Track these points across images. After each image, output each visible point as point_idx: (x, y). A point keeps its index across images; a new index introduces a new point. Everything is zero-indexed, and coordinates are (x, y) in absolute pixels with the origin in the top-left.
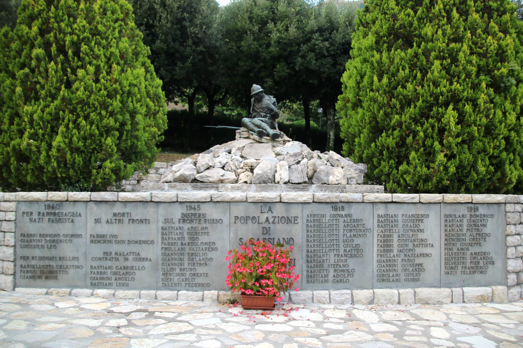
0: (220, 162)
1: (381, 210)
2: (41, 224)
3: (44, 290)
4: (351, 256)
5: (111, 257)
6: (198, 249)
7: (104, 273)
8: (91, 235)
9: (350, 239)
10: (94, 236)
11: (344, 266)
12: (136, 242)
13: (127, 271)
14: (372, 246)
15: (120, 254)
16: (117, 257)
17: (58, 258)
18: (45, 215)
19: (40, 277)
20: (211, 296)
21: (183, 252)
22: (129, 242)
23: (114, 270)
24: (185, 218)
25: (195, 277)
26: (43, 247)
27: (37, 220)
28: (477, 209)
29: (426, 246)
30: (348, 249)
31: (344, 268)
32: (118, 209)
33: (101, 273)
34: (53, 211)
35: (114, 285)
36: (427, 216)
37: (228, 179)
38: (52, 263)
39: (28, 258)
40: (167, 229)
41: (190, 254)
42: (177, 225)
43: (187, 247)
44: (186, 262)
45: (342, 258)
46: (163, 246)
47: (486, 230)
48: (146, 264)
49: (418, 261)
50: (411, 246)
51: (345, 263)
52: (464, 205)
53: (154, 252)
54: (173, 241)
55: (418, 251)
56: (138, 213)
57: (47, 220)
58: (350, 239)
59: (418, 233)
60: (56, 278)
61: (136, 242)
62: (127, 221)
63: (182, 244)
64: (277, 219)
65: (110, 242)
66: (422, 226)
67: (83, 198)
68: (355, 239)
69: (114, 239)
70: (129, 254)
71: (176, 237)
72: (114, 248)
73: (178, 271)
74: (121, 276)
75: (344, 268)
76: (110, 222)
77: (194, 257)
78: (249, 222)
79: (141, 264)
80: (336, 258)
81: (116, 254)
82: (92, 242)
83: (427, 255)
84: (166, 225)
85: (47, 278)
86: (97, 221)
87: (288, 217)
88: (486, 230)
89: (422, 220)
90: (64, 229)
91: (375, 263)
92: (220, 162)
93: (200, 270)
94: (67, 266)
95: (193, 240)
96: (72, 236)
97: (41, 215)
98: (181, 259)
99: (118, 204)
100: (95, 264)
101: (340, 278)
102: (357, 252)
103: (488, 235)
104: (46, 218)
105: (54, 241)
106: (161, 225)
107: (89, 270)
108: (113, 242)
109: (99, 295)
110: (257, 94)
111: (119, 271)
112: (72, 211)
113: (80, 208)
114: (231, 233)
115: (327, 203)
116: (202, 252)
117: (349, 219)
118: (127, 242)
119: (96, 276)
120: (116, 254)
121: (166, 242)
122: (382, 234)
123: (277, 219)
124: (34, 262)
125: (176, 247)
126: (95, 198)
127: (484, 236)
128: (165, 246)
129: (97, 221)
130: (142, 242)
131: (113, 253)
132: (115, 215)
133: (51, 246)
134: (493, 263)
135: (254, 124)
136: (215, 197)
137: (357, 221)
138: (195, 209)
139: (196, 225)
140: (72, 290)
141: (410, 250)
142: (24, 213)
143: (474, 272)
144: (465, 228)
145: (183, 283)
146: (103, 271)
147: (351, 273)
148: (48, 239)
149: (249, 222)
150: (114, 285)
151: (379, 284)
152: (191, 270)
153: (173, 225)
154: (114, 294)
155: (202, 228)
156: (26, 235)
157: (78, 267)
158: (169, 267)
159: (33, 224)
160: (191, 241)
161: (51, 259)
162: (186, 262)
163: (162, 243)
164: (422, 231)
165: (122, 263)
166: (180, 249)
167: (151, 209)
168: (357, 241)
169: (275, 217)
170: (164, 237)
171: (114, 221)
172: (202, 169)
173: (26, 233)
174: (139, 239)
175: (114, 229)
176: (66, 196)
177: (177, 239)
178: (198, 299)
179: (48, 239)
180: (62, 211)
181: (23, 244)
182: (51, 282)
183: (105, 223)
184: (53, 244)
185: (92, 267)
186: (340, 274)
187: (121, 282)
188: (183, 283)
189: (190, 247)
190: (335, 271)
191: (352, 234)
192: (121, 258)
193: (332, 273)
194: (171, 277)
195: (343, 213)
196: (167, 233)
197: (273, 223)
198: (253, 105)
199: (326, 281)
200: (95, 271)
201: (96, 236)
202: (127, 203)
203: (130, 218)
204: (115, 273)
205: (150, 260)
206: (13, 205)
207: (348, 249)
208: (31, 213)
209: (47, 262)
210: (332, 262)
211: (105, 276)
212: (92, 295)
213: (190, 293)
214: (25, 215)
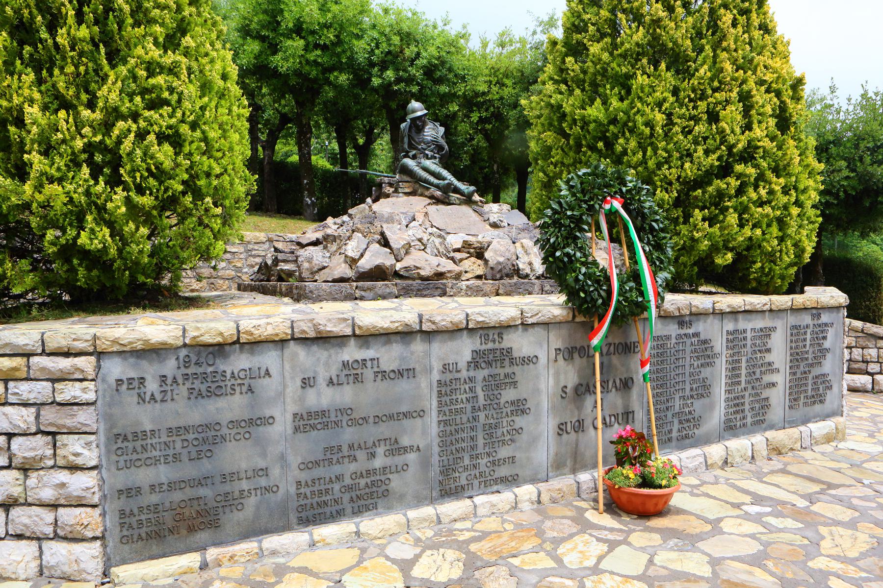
0: (420, 240)
1: (729, 326)
2: (169, 405)
3: (191, 560)
5: (340, 455)
6: (500, 415)
7: (327, 491)
8: (295, 415)
9: (697, 370)
10: (302, 418)
11: (690, 413)
12: (391, 417)
13: (373, 478)
14: (719, 377)
15: (360, 447)
16: (352, 453)
17: (218, 479)
20: (528, 497)
21: (474, 424)
22: (378, 420)
23: (348, 481)
24: (478, 360)
25: (496, 468)
26: (176, 458)
27: (158, 397)
28: (819, 316)
29: (772, 371)
30: (694, 386)
31: (690, 417)
32: (352, 353)
33: (320, 492)
34: (200, 370)
35: (349, 510)
36: (774, 329)
37: (449, 272)
38: (202, 492)
39: (139, 490)
40: (448, 383)
41: (487, 427)
42: (464, 374)
43: (482, 415)
44: (481, 442)
45: (689, 402)
46: (441, 418)
47: (827, 344)
48: (412, 457)
51: (691, 409)
52: (808, 311)
53: (425, 432)
54: (458, 407)
56: (389, 356)
57: (185, 393)
58: (697, 370)
59: (765, 355)
61: (391, 417)
62: (372, 376)
63: (473, 408)
64: (612, 348)
67: (277, 335)
68: (702, 369)
69: (345, 418)
70: (377, 444)
71: (464, 397)
72: (348, 435)
73: (467, 461)
74: (363, 492)
75: (690, 417)
76: (335, 381)
77: (494, 431)
78: (576, 355)
79: (399, 460)
80: (682, 402)
81: (351, 447)
82: (296, 429)
84: (448, 376)
85: (191, 530)
86: (307, 383)
87: (626, 344)
88: (827, 344)
89: (769, 335)
90: (230, 407)
91: (723, 404)
92: (420, 240)
93: (504, 452)
94: (242, 492)
96: (251, 422)
97: (169, 381)
98: (472, 438)
100: (304, 476)
101: (685, 432)
102: (704, 390)
103: (827, 350)
104: (183, 390)
106: (436, 376)
107: (293, 490)
108: (344, 423)
109: (328, 541)
110: (420, 117)
111: (357, 481)
112: (247, 367)
113: (270, 359)
114: (551, 379)
115: (674, 317)
116: (507, 419)
117: (696, 339)
118: (371, 420)
119: (308, 502)
120: (351, 447)
121: (446, 409)
122: (730, 359)
123: (612, 348)
124: (154, 498)
125: (463, 416)
126: (304, 332)
127: (824, 352)
128: (444, 418)
129: (307, 383)
130: (401, 416)
131: (345, 448)
132: (345, 365)
135: (426, 169)
136: (529, 315)
137: (705, 342)
138: (494, 341)
139: (497, 371)
140: (260, 542)
141: (757, 379)
142: (119, 382)
143: (814, 403)
144: (808, 343)
145: (476, 482)
146: (322, 487)
147: (697, 422)
148: (191, 437)
149: (576, 355)
150: (349, 510)
151: (726, 434)
152: (488, 455)
153: (458, 375)
154: (358, 533)
155: (507, 376)
156: (130, 437)
158: (451, 457)
159: (149, 407)
160: (489, 402)
161: (203, 481)
162: (481, 442)
163: (439, 412)
165: (362, 463)
166: (471, 419)
167: (418, 346)
168: (706, 372)
169: (610, 344)
170: (443, 399)
171: (343, 379)
172: (403, 251)
173: (129, 431)
174: (395, 411)
175: (346, 395)
176: (235, 332)
177: (464, 400)
178: (509, 507)
179: (191, 437)
180: (222, 367)
182: (202, 536)
183: (324, 384)
184: (205, 447)
185: (299, 483)
186: (685, 426)
187: (362, 502)
188: (476, 482)
189: (487, 412)
190: (680, 422)
191: (699, 362)
192: (361, 455)
193: (676, 426)
194: (455, 475)
195: (691, 331)
196: (448, 392)
197: (607, 354)
198: (409, 136)
199: (670, 440)
201: (305, 417)
202: (370, 339)
203: (376, 370)
204: (349, 488)
205: (418, 449)
206: (86, 363)
207: (694, 386)
209: (190, 493)
210: (677, 409)
212: (313, 545)
213: (494, 498)
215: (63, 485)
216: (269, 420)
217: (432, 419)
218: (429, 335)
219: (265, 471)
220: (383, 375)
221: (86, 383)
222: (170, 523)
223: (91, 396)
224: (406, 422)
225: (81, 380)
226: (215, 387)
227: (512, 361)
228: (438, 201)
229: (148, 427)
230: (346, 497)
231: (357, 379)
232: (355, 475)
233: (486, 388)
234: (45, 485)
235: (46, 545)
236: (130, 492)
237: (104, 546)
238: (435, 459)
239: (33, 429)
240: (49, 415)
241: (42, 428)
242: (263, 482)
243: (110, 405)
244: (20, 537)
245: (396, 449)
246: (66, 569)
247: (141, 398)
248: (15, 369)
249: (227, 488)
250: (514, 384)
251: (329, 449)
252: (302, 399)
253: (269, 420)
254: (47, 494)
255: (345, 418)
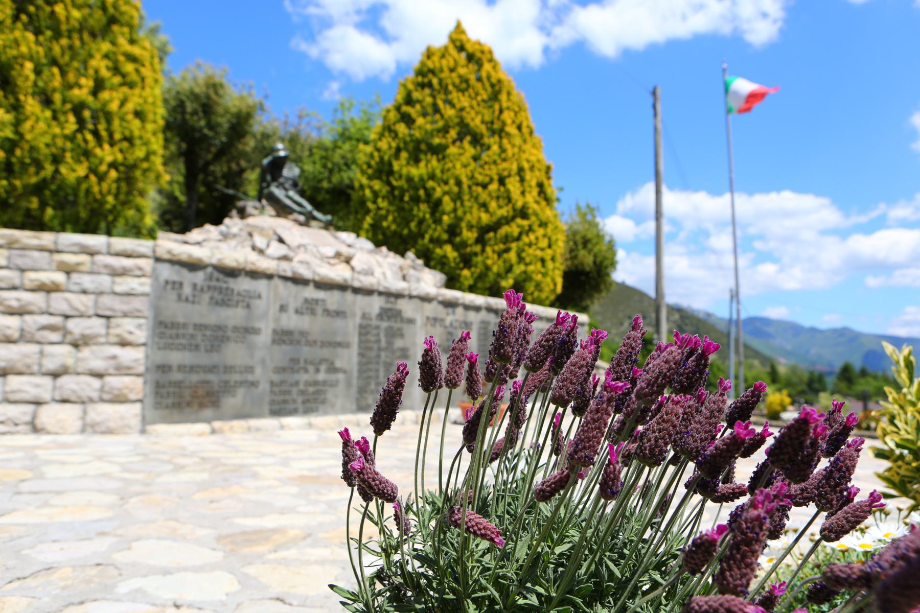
17: (222, 369)
18: (205, 289)
19: (189, 404)
23: (302, 387)
26: (197, 347)
27: (191, 298)
32: (310, 292)
38: (212, 377)
43: (383, 354)
48: (341, 376)
56: (332, 299)
60: (216, 404)
72: (305, 352)
79: (333, 377)
81: (306, 361)
82: (274, 342)
84: (365, 322)
85: (202, 406)
90: (233, 316)
95: (390, 343)
99: (311, 286)
100: (276, 378)
104: (206, 297)
105: (216, 338)
106: (358, 320)
113: (261, 285)
118: (319, 344)
124: (177, 376)
126: (284, 271)
129: (283, 308)
131: (302, 362)
132: (306, 301)
133: (212, 346)
142: (167, 282)
148: (208, 333)
157: (254, 384)
159: (183, 305)
161: (212, 369)
167: (349, 296)
171: (304, 311)
181: (163, 341)
182: (208, 412)
184: (216, 343)
192: (311, 368)
200: (276, 389)
204: (303, 393)
208: (181, 284)
211: (287, 397)
214: (169, 287)
215: (114, 357)
216: (256, 331)
217: (355, 349)
218: (356, 291)
219: (250, 369)
220: (327, 312)
221: (143, 280)
222: (188, 398)
223: (147, 289)
224: (340, 350)
225: (139, 276)
226: (225, 300)
227: (402, 320)
228: (301, 224)
229: (181, 320)
230: (300, 399)
231: (313, 312)
232: (308, 384)
233: (387, 335)
234: (93, 358)
235: (91, 408)
236: (163, 368)
237: (143, 409)
238: (355, 381)
239: (91, 312)
240: (106, 300)
241: (101, 312)
242: (250, 378)
243: (159, 298)
244: (65, 401)
245: (333, 369)
246: (112, 425)
247: (179, 297)
248: (79, 264)
249: (226, 377)
250: (402, 336)
251: (295, 361)
252: (277, 320)
253: (256, 331)
254: (98, 364)
255: (303, 340)
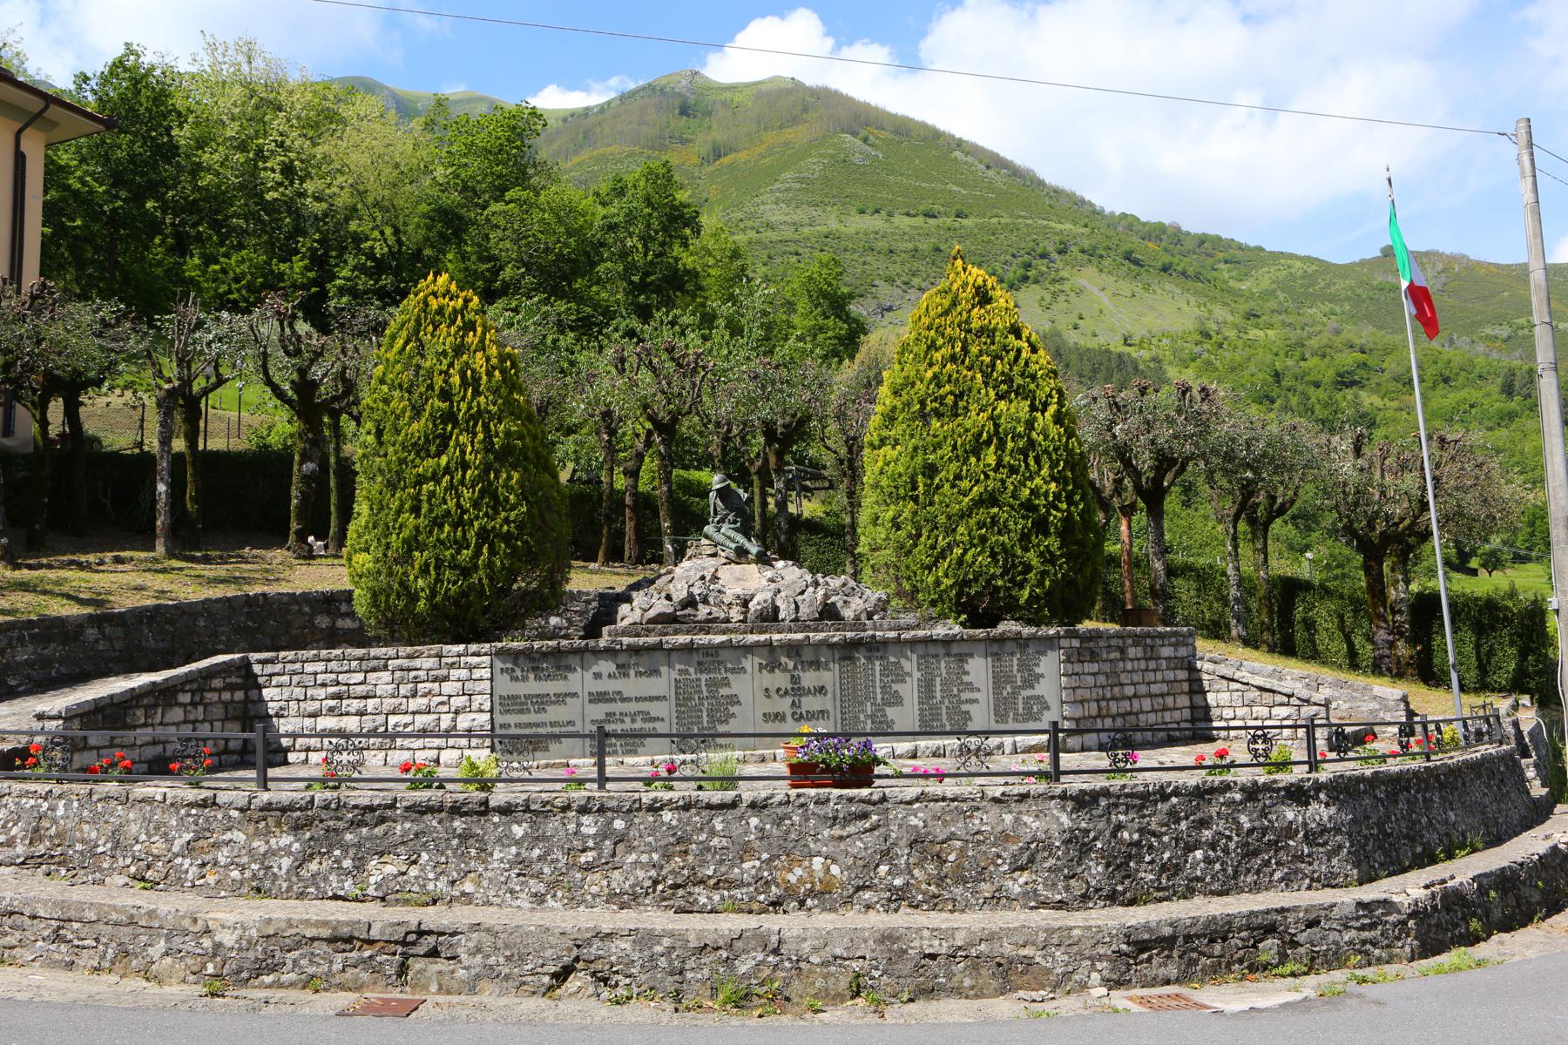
4: (890, 705)
22: (638, 699)
29: (972, 690)
49: (964, 707)
50: (955, 691)
55: (964, 696)
61: (645, 699)
65: (614, 700)
66: (967, 667)
83: (976, 701)
95: (713, 695)
103: (1042, 676)
134: (1048, 708)
161: (538, 725)
164: (967, 673)
168: (895, 687)
192: (627, 720)
250: (728, 685)
